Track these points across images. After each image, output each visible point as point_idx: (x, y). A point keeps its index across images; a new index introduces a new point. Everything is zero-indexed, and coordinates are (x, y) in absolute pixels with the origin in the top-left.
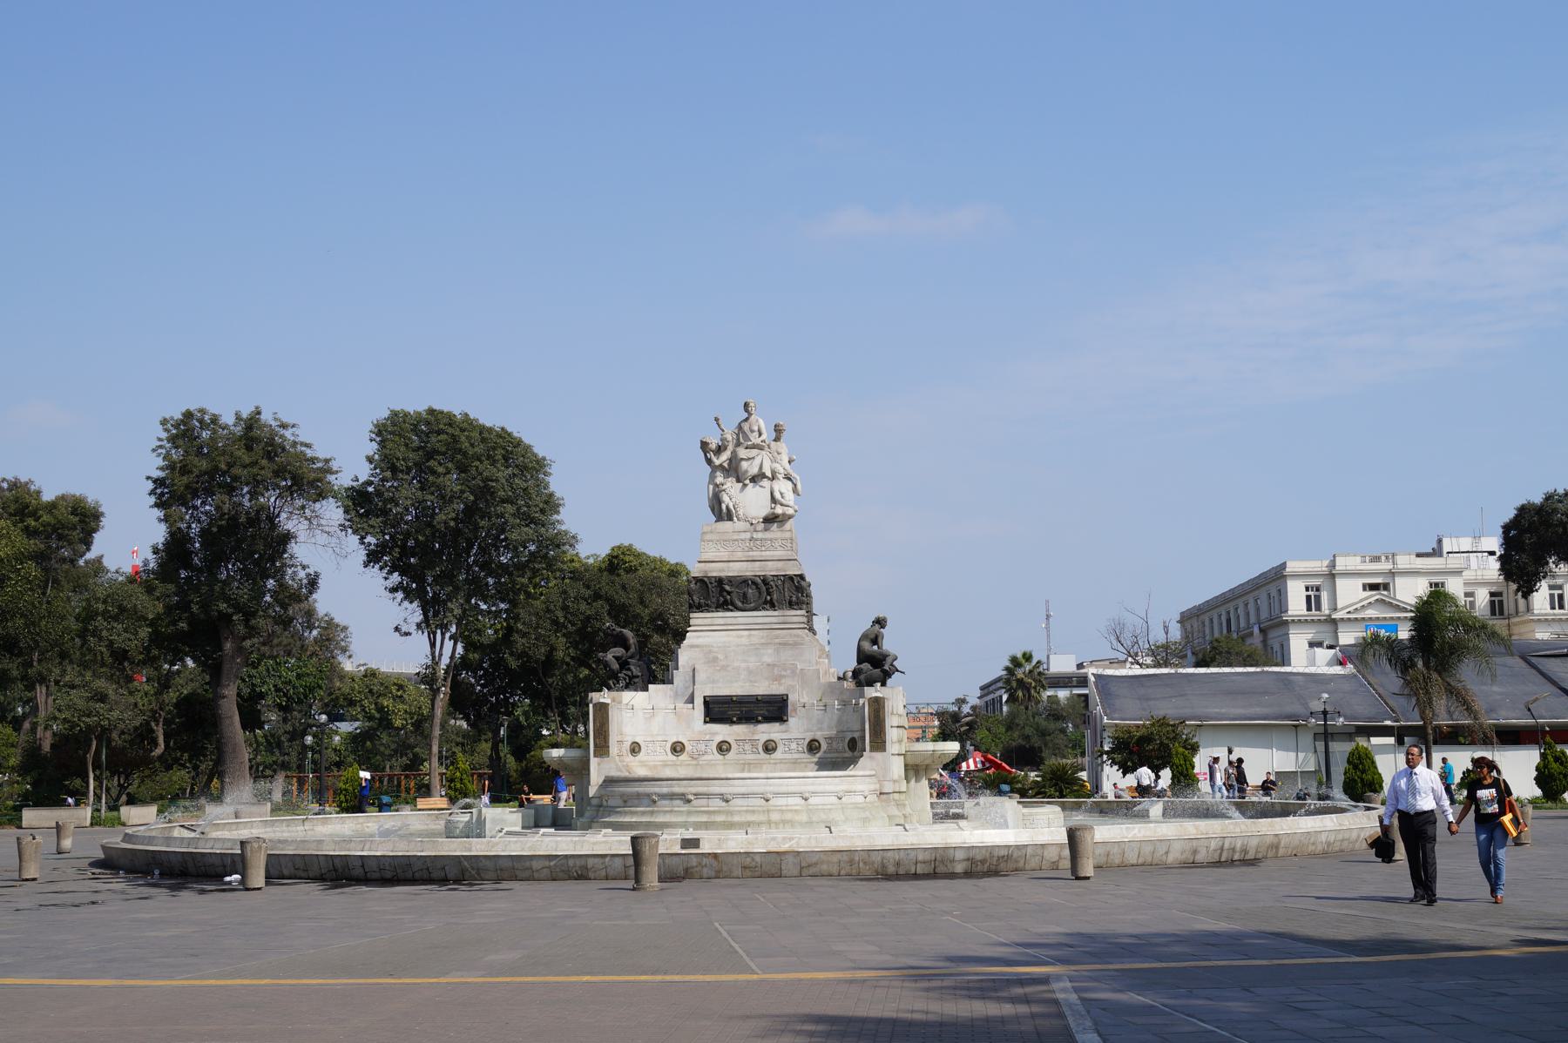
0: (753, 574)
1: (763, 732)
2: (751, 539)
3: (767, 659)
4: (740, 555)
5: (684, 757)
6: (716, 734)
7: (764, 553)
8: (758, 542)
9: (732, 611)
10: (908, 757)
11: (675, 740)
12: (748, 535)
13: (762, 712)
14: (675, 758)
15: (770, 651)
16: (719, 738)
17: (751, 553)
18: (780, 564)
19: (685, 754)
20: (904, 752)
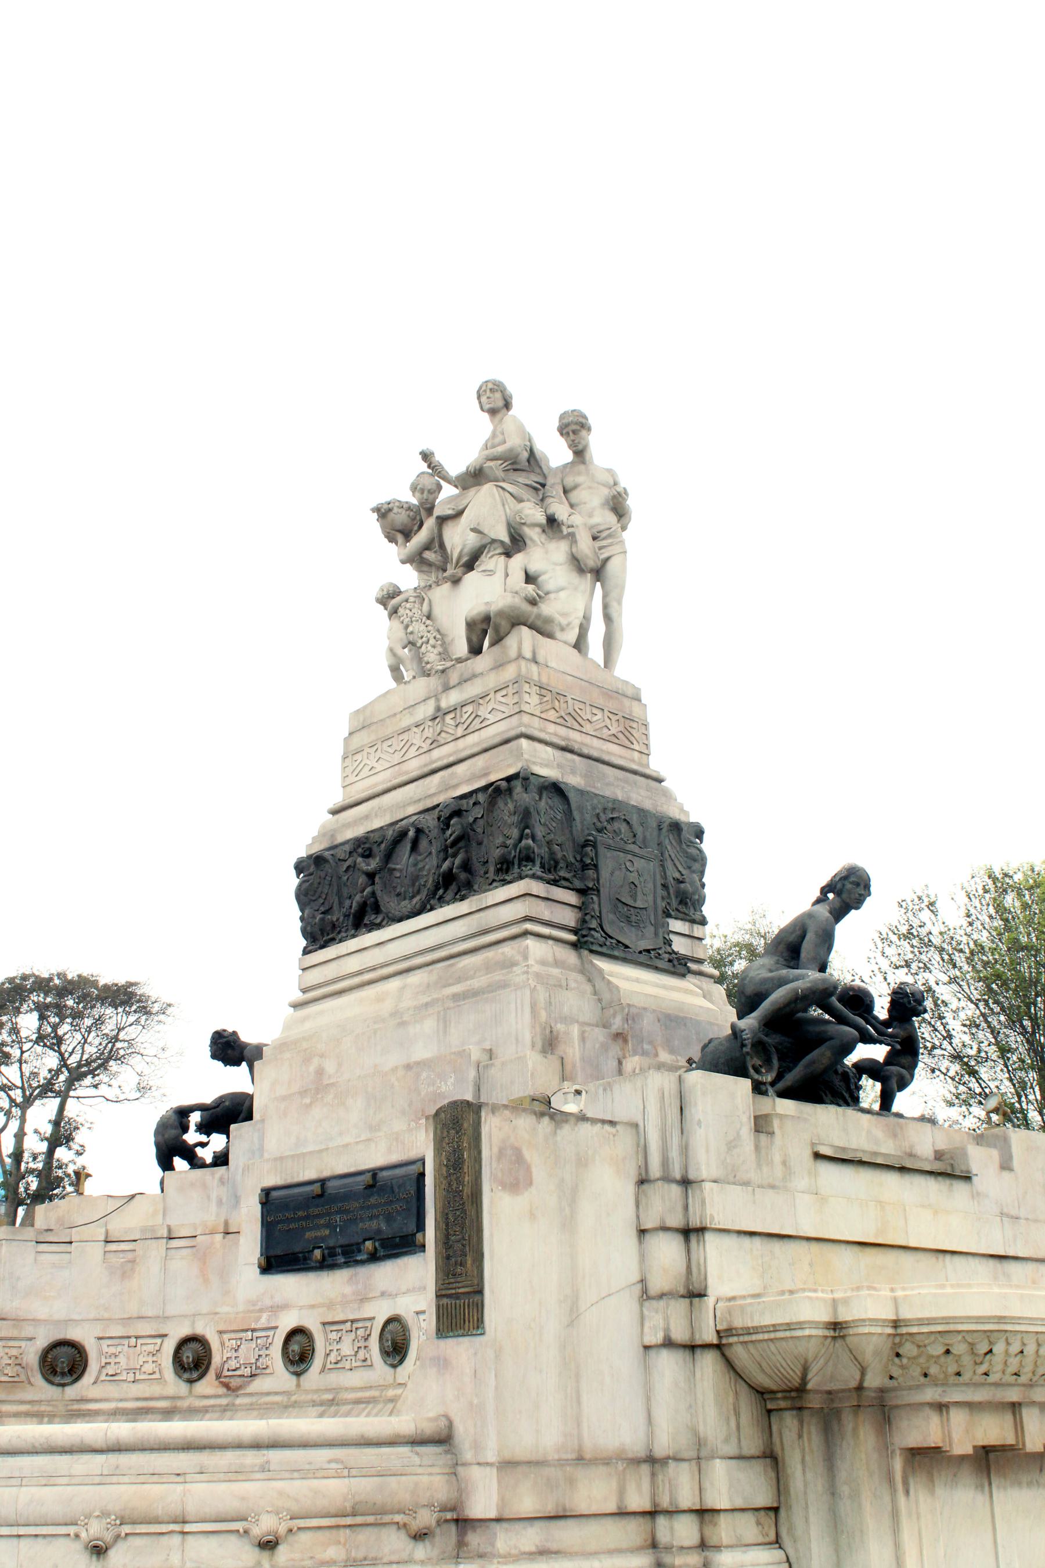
0: (421, 807)
1: (383, 1294)
2: (439, 715)
3: (421, 1052)
4: (414, 767)
5: (207, 1385)
6: (285, 1307)
7: (461, 743)
8: (448, 718)
9: (379, 926)
10: (740, 1354)
11: (185, 1331)
12: (429, 709)
13: (374, 1224)
14: (183, 1388)
15: (429, 1025)
16: (288, 1322)
17: (436, 753)
18: (480, 762)
19: (211, 1374)
20: (711, 1337)
